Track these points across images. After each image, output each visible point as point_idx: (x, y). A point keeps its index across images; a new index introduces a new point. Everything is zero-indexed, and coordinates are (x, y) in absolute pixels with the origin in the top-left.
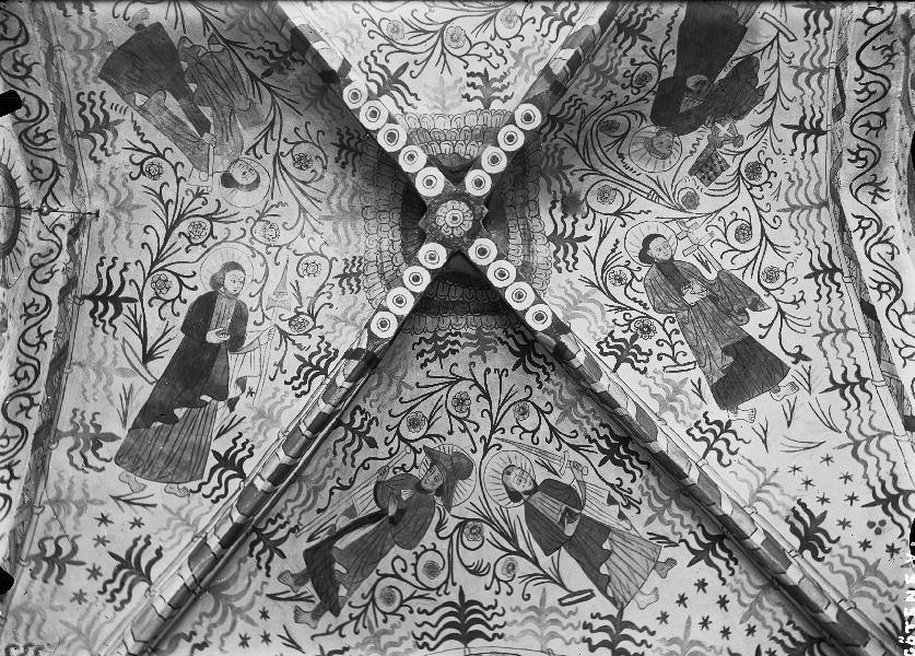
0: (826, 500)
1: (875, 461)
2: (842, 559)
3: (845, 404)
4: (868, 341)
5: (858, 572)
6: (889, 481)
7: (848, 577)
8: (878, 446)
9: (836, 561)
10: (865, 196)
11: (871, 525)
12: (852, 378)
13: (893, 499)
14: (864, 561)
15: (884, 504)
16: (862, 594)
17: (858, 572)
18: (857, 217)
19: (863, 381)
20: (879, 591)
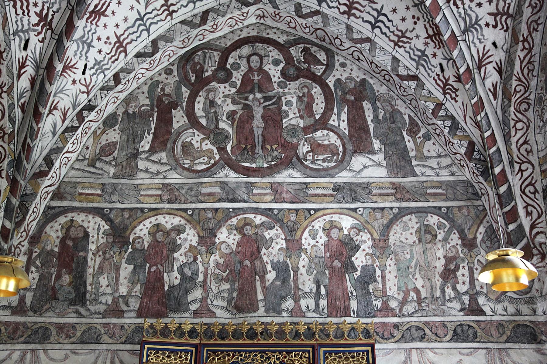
0: (114, 15)
1: (136, 31)
2: (90, 31)
3: (158, 8)
4: (189, 14)
5: (87, 40)
6: (128, 40)
7: (83, 36)
8: (143, 30)
9: (88, 29)
10: (258, 12)
11: (108, 38)
12: (172, 8)
13: (121, 45)
14: (92, 41)
15: (118, 41)
16: (78, 44)
17: (87, 40)
18: (248, 12)
19: (171, 14)
20: (82, 51)
